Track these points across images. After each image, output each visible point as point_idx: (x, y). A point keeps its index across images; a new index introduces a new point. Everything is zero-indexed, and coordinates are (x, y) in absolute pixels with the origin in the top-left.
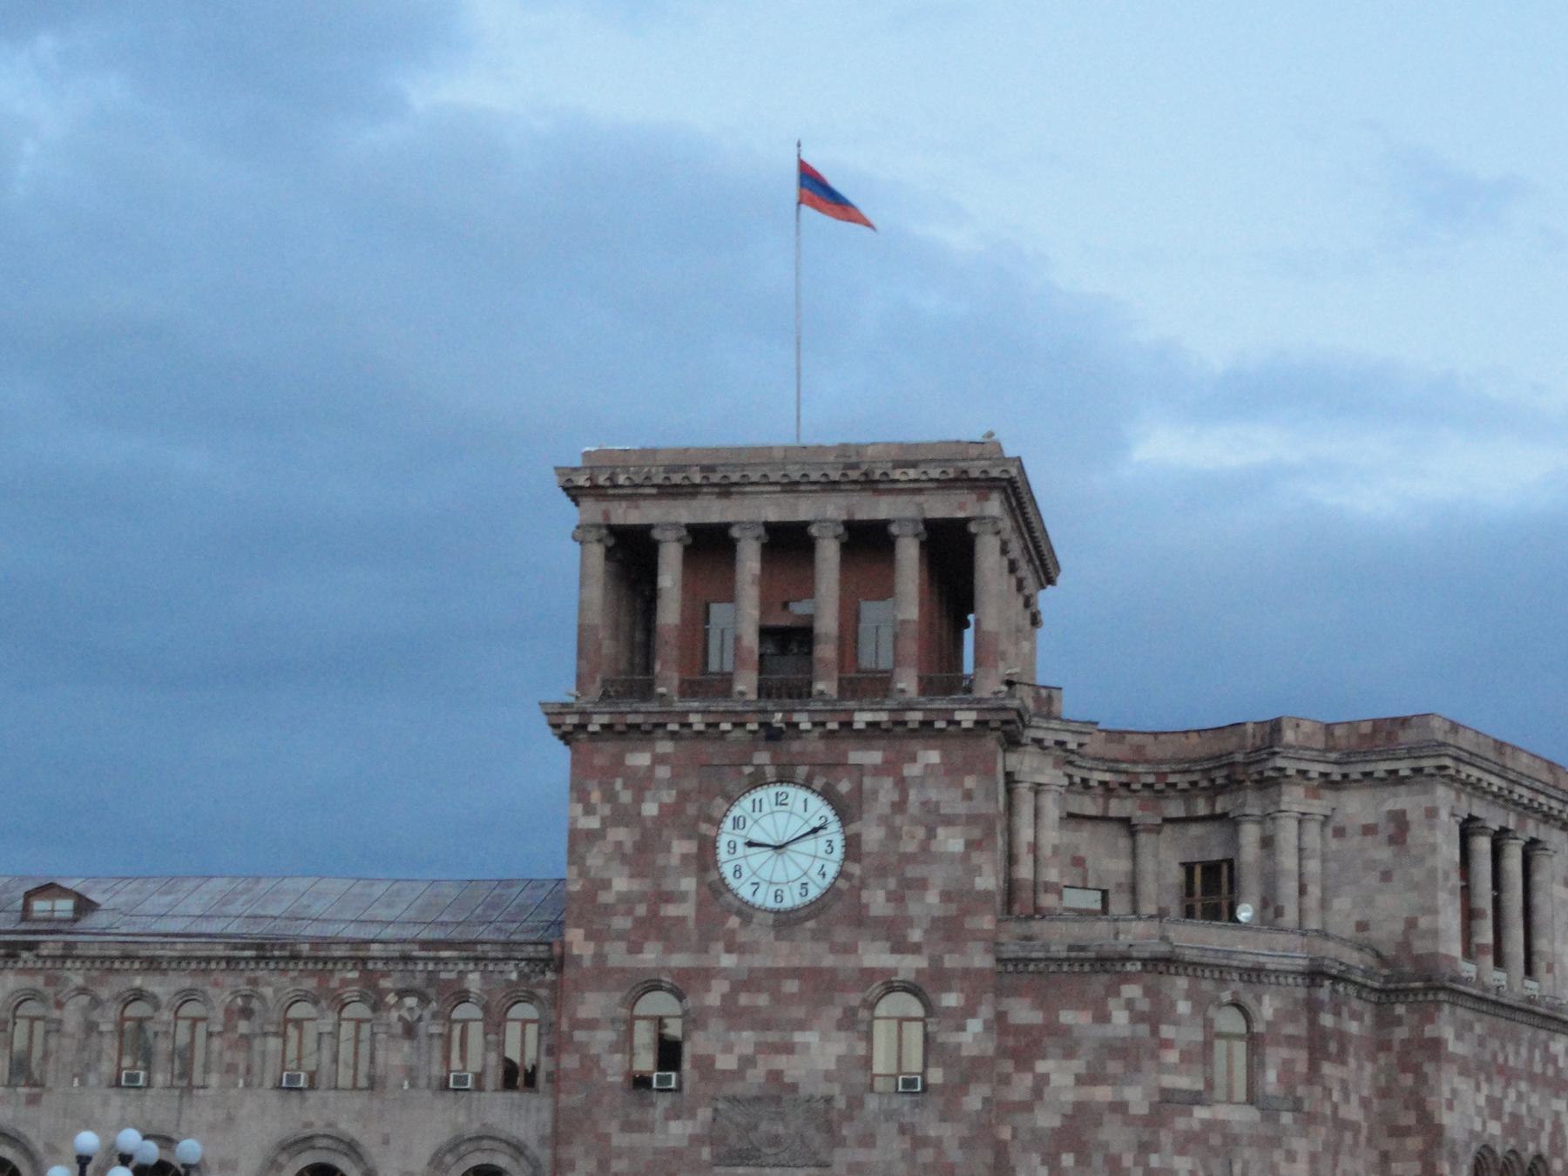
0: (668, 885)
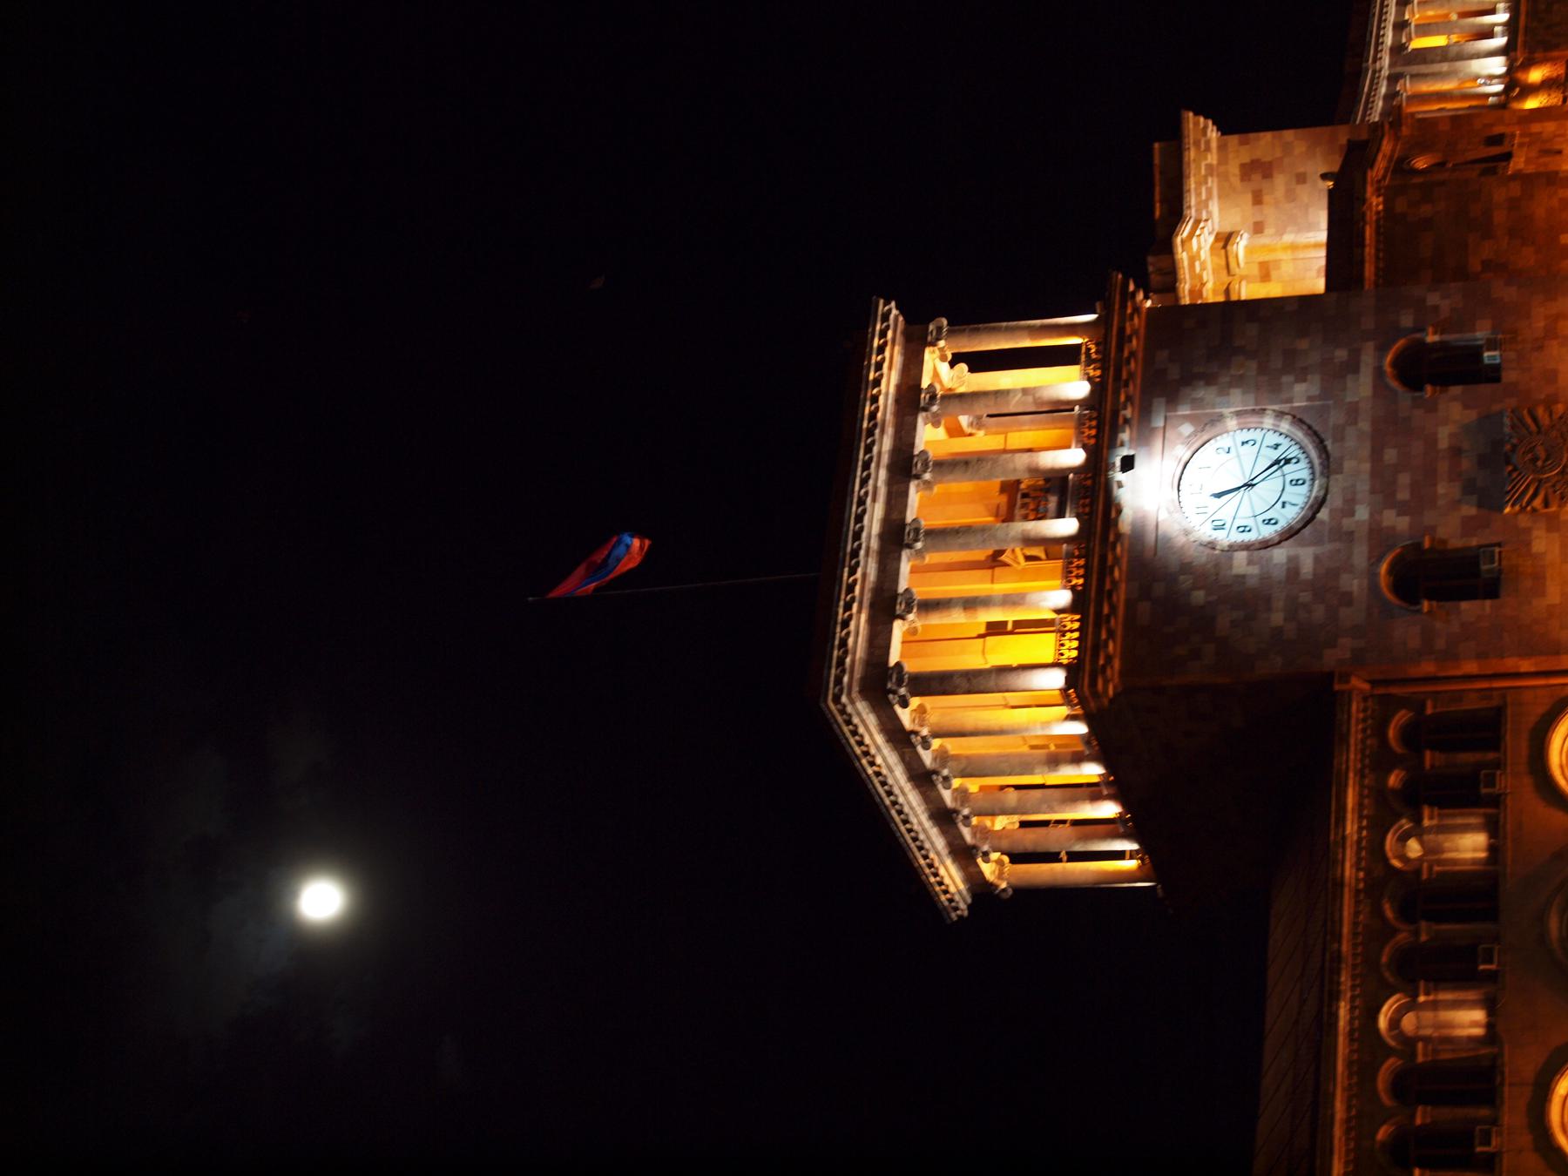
0: (1279, 574)
